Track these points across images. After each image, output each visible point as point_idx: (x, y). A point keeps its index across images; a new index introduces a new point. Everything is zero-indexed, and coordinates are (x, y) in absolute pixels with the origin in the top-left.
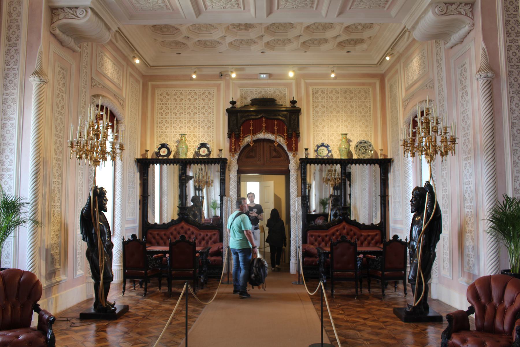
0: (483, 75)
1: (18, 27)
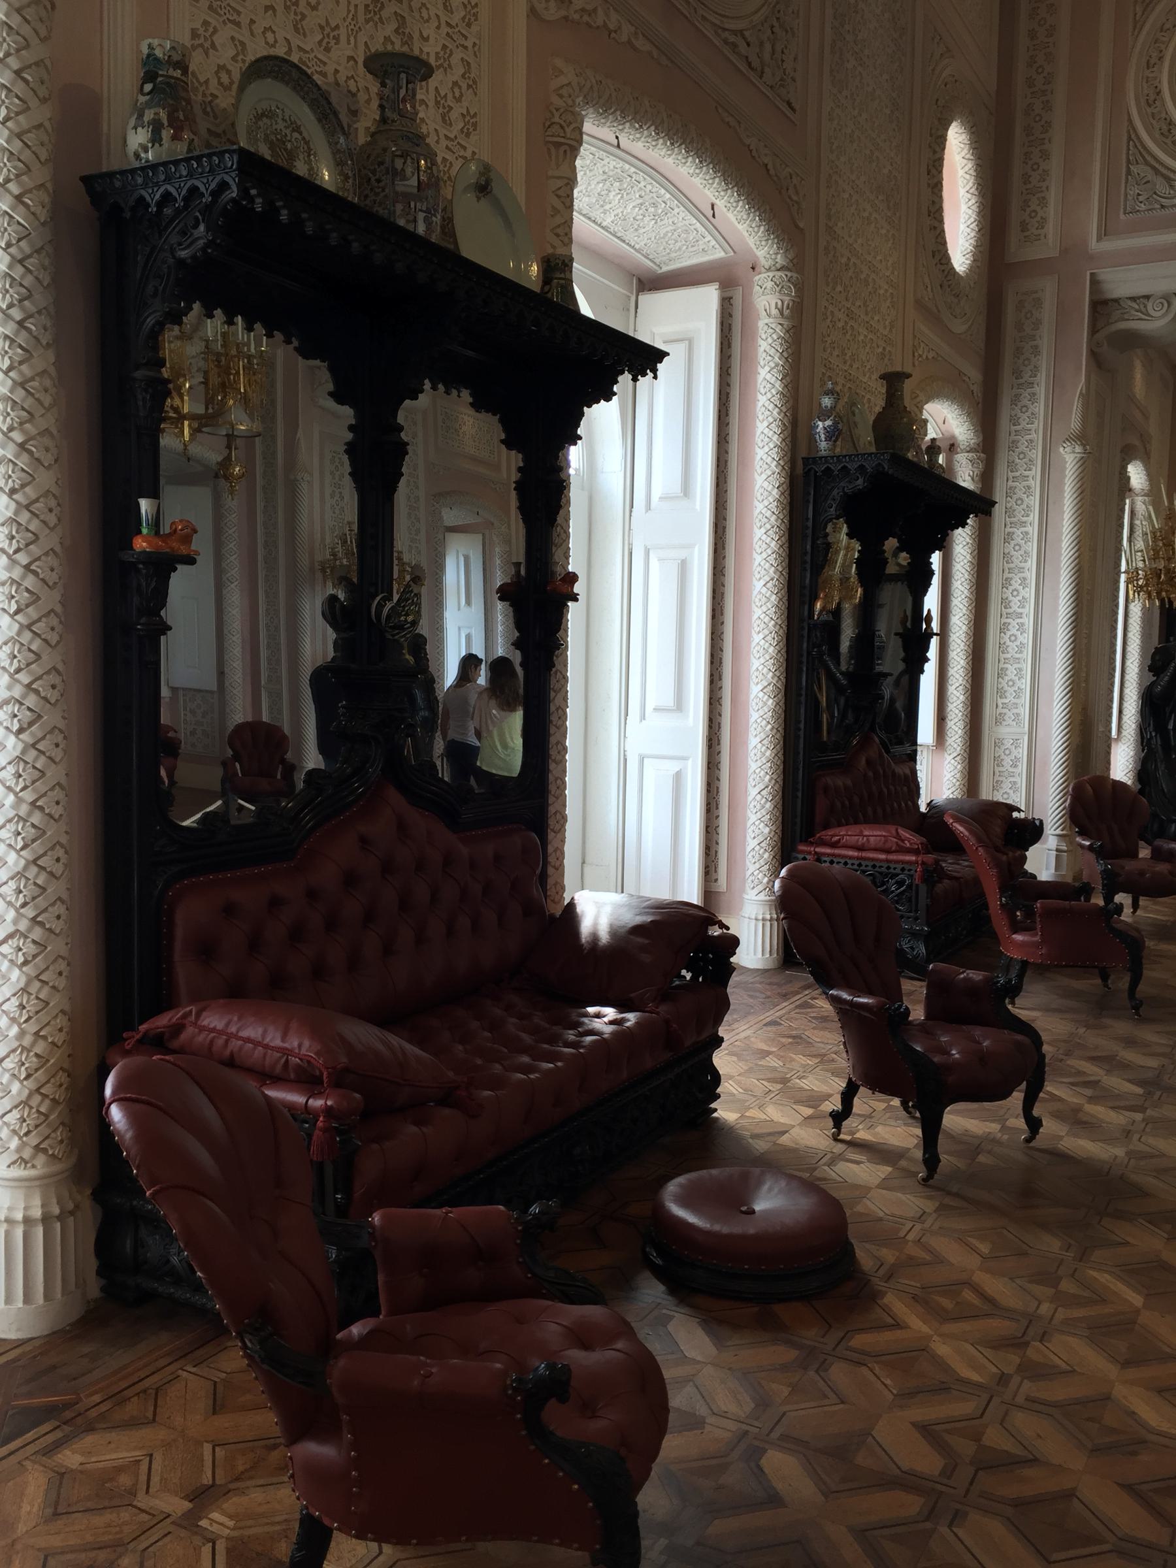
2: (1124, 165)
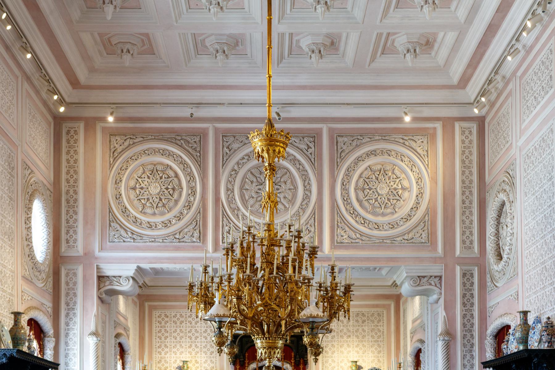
0: (441, 339)
1: (75, 295)
2: (108, 222)
